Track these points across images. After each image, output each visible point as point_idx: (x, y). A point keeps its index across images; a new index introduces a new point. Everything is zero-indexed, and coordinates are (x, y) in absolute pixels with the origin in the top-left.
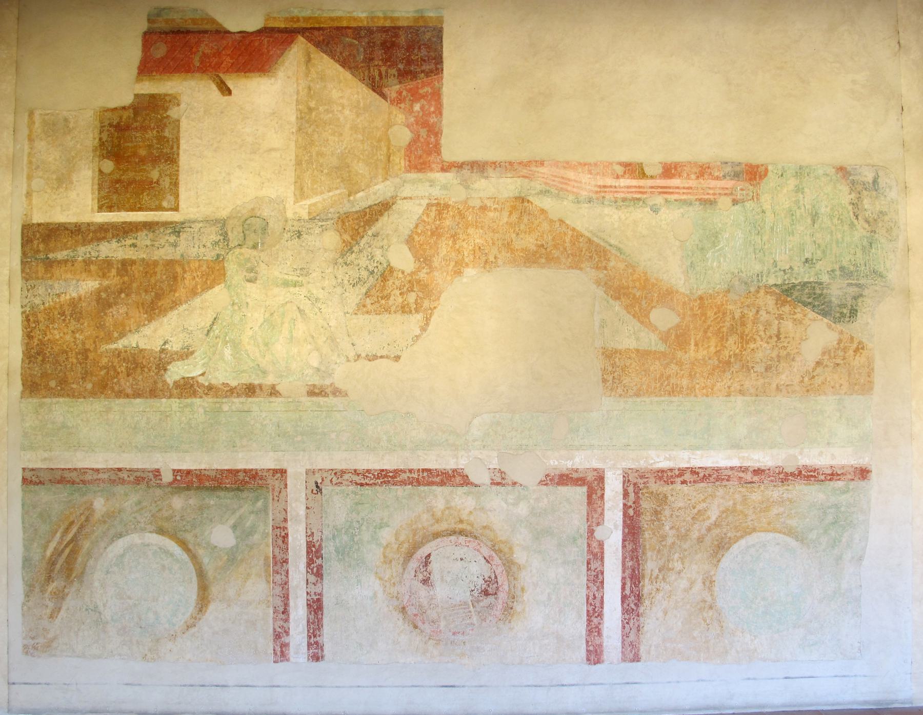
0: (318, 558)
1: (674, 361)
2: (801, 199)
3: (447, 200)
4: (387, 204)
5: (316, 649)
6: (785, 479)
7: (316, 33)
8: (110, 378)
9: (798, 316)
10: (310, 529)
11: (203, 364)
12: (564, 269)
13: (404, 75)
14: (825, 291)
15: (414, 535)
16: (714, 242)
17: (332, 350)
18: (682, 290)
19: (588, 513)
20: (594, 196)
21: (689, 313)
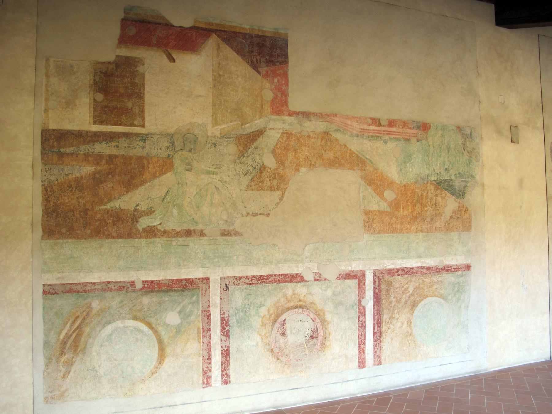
0: (227, 326)
1: (394, 216)
2: (444, 140)
3: (291, 131)
4: (262, 131)
5: (226, 377)
6: (439, 272)
7: (223, 33)
8: (102, 227)
9: (443, 195)
10: (223, 310)
11: (160, 218)
12: (346, 170)
13: (269, 62)
14: (453, 184)
15: (277, 310)
16: (410, 159)
17: (234, 211)
18: (397, 182)
19: (358, 293)
20: (359, 134)
21: (400, 193)
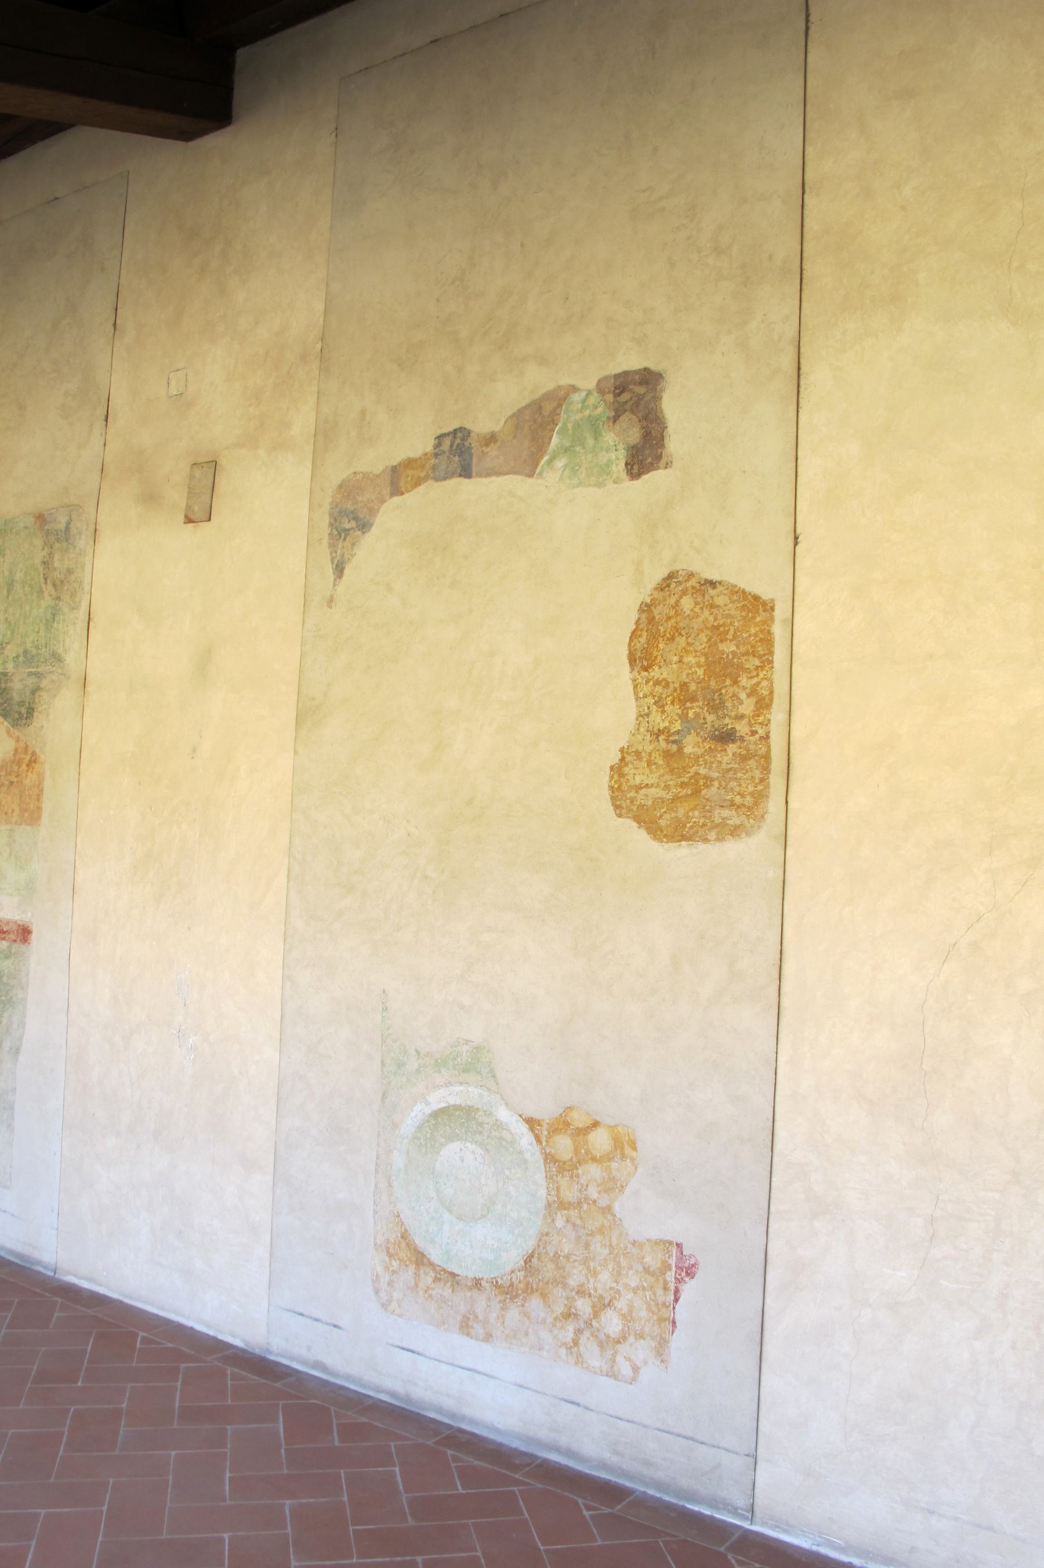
14: (9, 685)
